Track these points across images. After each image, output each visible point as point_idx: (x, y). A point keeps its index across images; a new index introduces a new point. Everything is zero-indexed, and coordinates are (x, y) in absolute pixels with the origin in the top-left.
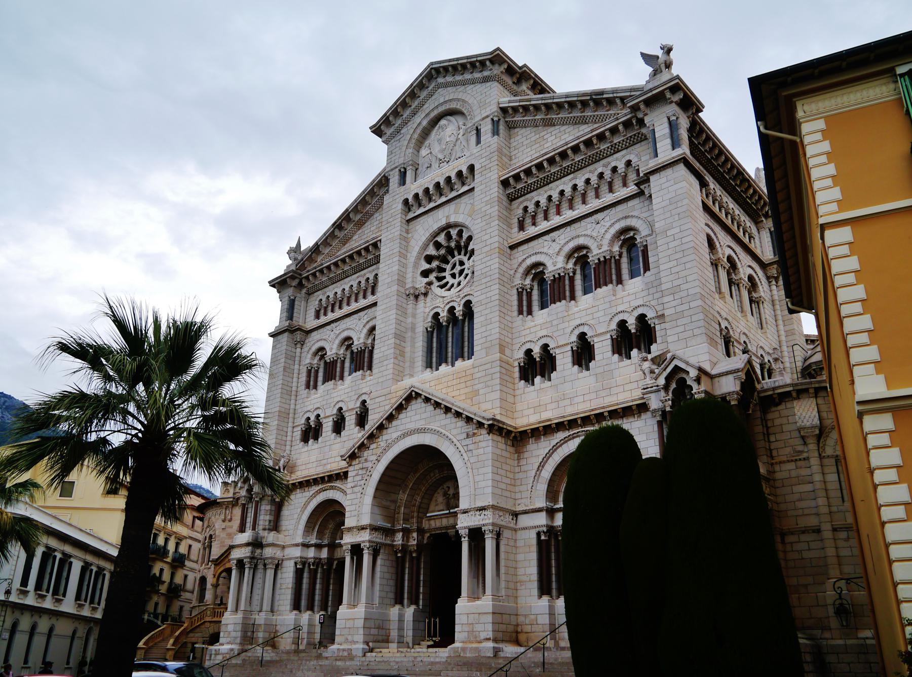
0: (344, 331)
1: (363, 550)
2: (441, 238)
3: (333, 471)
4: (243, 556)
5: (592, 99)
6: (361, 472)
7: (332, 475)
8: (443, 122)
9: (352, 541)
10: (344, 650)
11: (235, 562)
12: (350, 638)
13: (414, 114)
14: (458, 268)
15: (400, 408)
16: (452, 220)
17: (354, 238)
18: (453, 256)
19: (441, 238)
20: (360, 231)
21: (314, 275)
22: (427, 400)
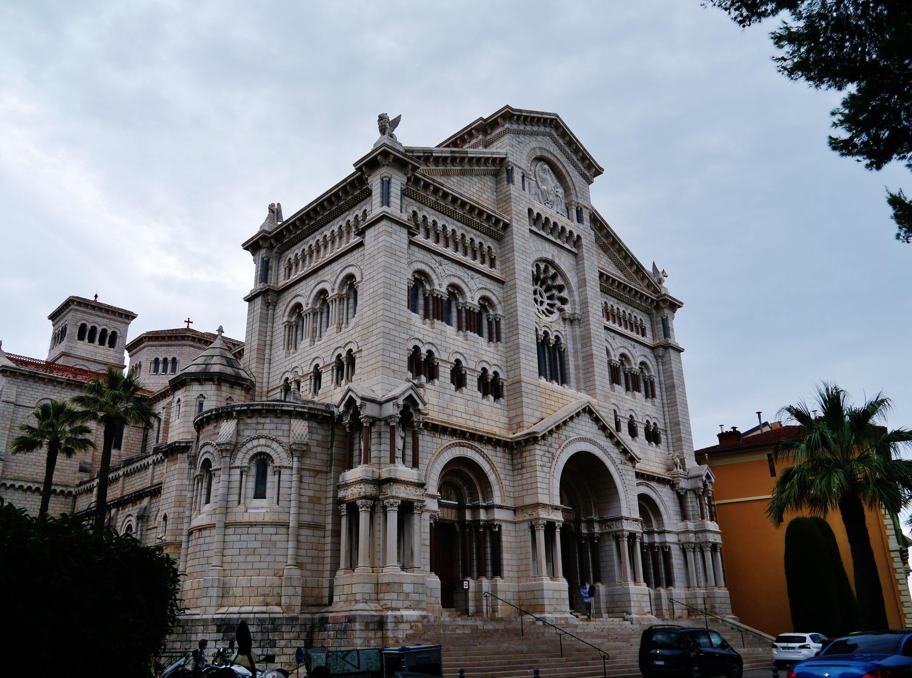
0: (455, 276)
1: (555, 528)
2: (542, 266)
3: (479, 431)
4: (414, 498)
5: (637, 266)
6: (547, 454)
7: (475, 434)
8: (546, 167)
9: (549, 517)
10: (561, 619)
11: (400, 502)
12: (558, 607)
13: (532, 134)
14: (538, 296)
15: (578, 414)
16: (557, 261)
17: (452, 179)
18: (536, 285)
19: (542, 266)
20: (459, 178)
21: (427, 186)
22: (597, 420)
